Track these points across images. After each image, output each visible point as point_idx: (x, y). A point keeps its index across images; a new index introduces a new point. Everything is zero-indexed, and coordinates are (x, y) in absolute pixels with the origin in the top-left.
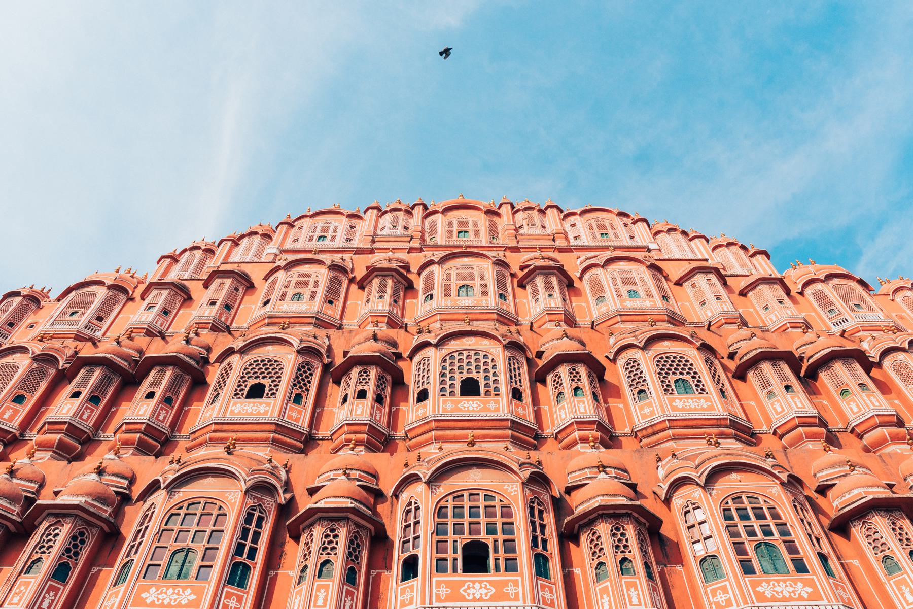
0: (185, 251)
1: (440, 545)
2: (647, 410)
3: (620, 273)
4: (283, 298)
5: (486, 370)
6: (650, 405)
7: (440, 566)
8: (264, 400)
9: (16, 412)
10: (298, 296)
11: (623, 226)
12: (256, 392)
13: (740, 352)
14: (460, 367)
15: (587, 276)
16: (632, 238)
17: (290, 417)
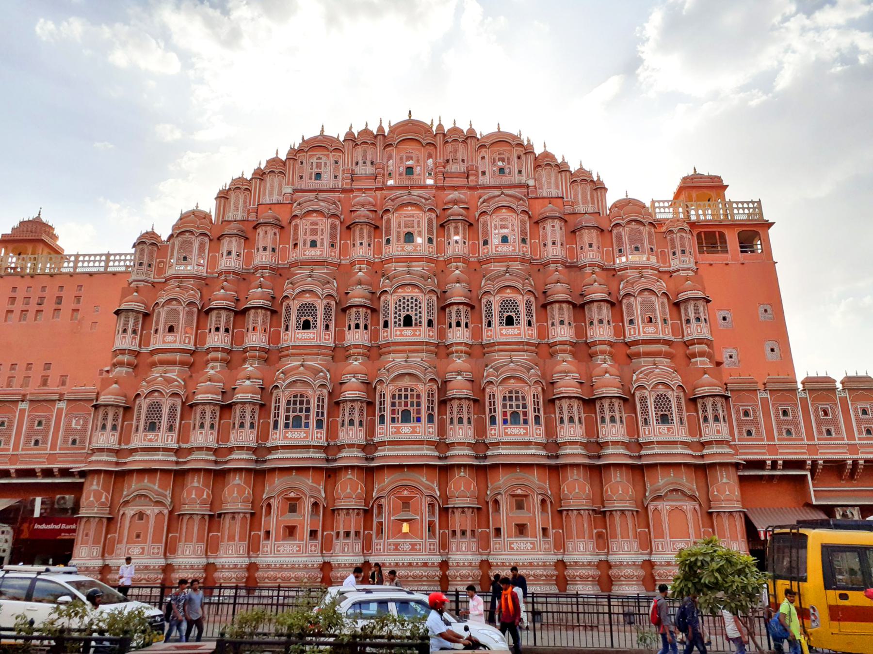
0: (230, 189)
1: (393, 412)
2: (489, 333)
3: (501, 220)
4: (305, 245)
5: (416, 310)
6: (491, 331)
7: (393, 420)
8: (311, 330)
9: (190, 338)
10: (313, 244)
11: (516, 159)
12: (306, 325)
13: (548, 293)
14: (404, 308)
15: (481, 220)
16: (520, 172)
17: (325, 339)
